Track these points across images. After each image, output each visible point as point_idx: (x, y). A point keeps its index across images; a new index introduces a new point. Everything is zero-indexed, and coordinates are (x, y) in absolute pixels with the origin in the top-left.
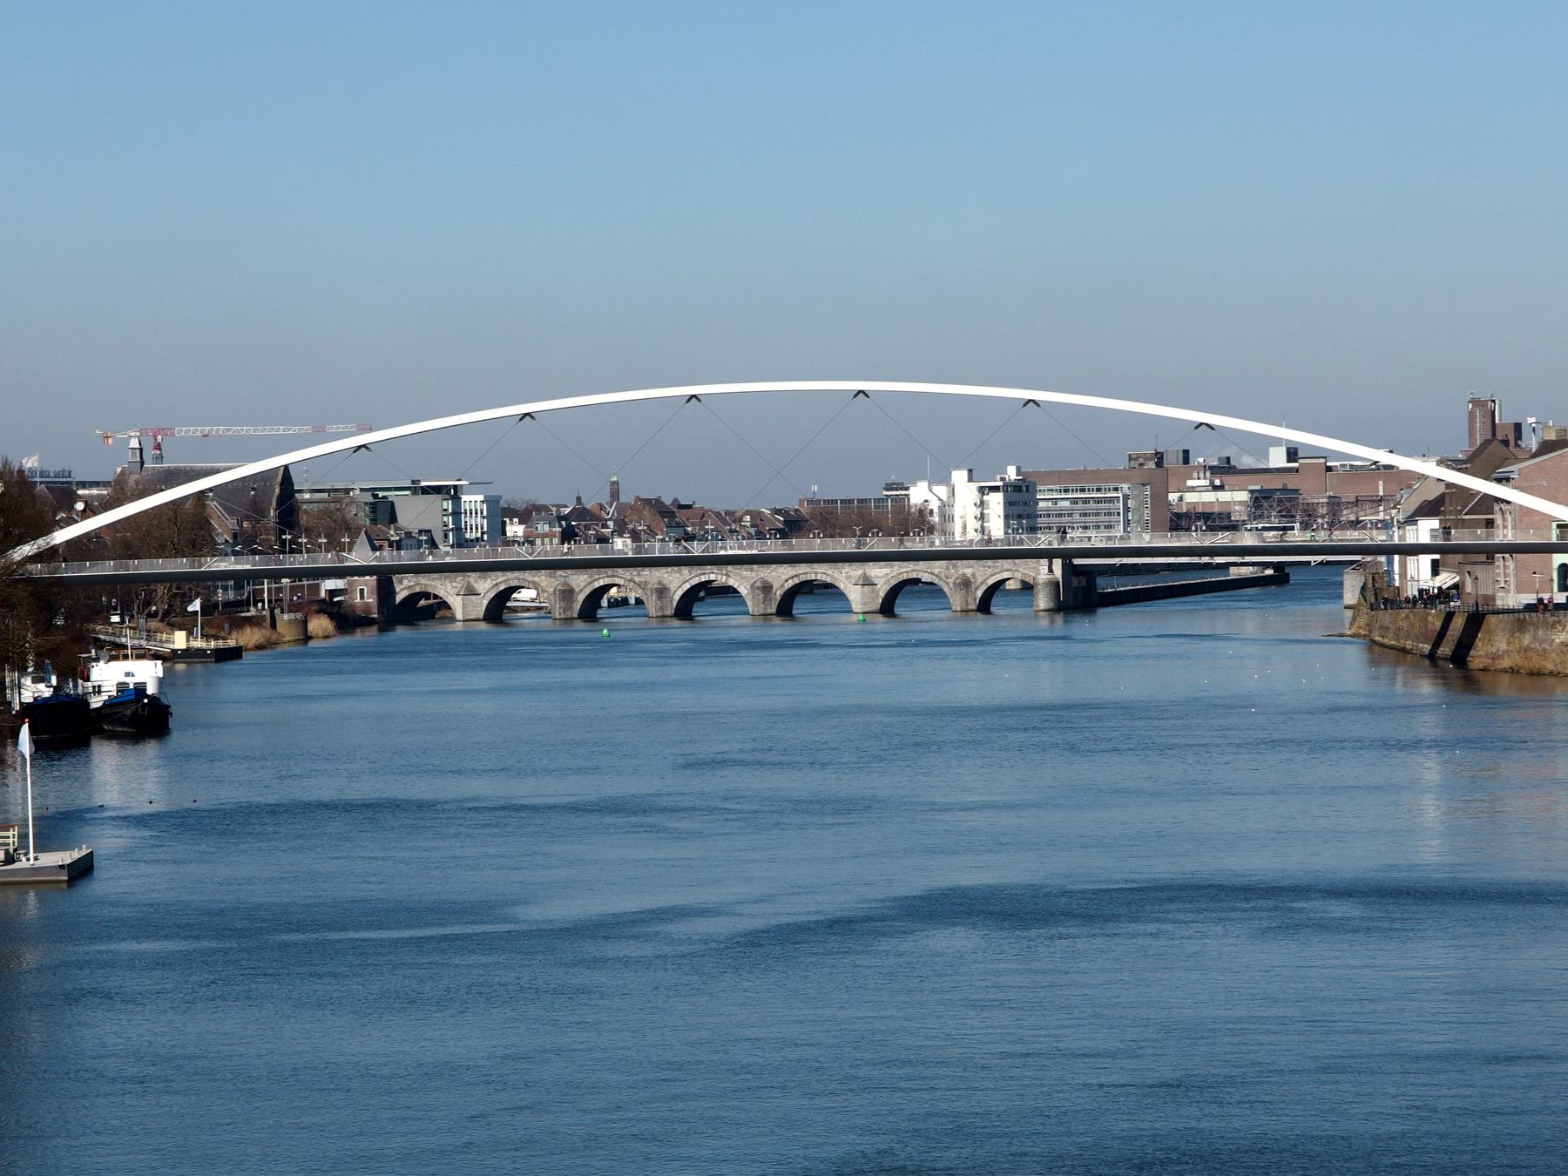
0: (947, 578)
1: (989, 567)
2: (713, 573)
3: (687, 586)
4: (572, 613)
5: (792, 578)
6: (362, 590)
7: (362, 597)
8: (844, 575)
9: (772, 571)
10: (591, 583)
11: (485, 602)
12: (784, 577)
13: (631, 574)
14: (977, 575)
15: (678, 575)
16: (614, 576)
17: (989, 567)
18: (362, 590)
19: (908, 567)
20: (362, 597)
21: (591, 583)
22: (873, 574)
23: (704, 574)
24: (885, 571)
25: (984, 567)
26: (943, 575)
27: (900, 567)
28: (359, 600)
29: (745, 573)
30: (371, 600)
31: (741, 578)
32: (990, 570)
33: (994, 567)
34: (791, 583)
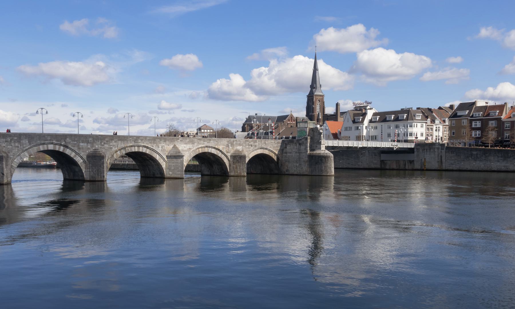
0: (227, 153)
1: (251, 145)
2: (52, 143)
5: (120, 150)
8: (160, 148)
9: (104, 143)
12: (114, 149)
15: (17, 144)
17: (251, 145)
19: (203, 144)
23: (44, 144)
24: (189, 146)
25: (249, 145)
27: (199, 144)
29: (81, 144)
31: (79, 148)
32: (252, 148)
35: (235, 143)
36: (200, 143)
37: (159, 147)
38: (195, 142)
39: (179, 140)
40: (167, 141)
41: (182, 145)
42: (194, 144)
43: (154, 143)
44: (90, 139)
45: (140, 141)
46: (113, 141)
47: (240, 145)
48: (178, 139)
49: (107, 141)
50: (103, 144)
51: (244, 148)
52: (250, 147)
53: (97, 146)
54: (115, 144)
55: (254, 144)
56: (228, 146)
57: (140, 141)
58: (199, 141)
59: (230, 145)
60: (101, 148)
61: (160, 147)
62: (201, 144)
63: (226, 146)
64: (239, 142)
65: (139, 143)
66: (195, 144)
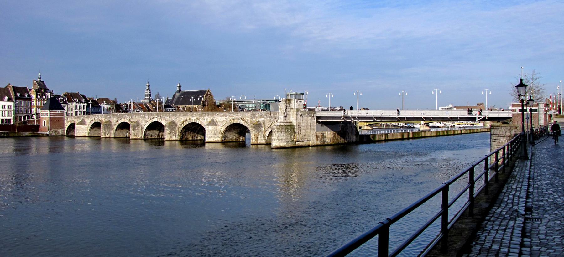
2: (156, 118)
3: (148, 124)
4: (110, 135)
5: (186, 120)
6: (44, 122)
7: (45, 125)
10: (117, 121)
11: (89, 128)
12: (182, 121)
13: (130, 117)
14: (266, 122)
16: (124, 118)
18: (44, 122)
19: (233, 117)
20: (45, 125)
21: (117, 121)
22: (217, 121)
23: (153, 118)
24: (224, 118)
26: (249, 122)
27: (230, 116)
28: (43, 126)
29: (167, 118)
30: (47, 126)
32: (272, 120)
33: (274, 117)
34: (185, 124)
35: (257, 115)
36: (230, 116)
37: (205, 119)
38: (227, 116)
39: (217, 114)
40: (209, 115)
41: (219, 118)
42: (227, 117)
43: (202, 117)
44: (171, 115)
45: (194, 115)
46: (181, 116)
47: (261, 117)
48: (216, 113)
49: (178, 116)
50: (176, 117)
51: (265, 119)
52: (270, 118)
53: (174, 119)
54: (182, 117)
55: (274, 116)
56: (252, 118)
57: (194, 115)
58: (230, 114)
59: (253, 117)
60: (175, 120)
61: (205, 119)
62: (231, 117)
63: (250, 118)
64: (261, 115)
65: (194, 117)
66: (227, 117)
